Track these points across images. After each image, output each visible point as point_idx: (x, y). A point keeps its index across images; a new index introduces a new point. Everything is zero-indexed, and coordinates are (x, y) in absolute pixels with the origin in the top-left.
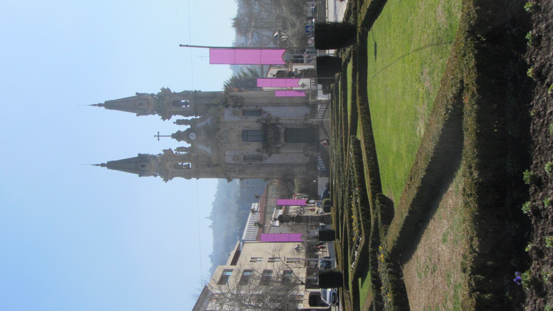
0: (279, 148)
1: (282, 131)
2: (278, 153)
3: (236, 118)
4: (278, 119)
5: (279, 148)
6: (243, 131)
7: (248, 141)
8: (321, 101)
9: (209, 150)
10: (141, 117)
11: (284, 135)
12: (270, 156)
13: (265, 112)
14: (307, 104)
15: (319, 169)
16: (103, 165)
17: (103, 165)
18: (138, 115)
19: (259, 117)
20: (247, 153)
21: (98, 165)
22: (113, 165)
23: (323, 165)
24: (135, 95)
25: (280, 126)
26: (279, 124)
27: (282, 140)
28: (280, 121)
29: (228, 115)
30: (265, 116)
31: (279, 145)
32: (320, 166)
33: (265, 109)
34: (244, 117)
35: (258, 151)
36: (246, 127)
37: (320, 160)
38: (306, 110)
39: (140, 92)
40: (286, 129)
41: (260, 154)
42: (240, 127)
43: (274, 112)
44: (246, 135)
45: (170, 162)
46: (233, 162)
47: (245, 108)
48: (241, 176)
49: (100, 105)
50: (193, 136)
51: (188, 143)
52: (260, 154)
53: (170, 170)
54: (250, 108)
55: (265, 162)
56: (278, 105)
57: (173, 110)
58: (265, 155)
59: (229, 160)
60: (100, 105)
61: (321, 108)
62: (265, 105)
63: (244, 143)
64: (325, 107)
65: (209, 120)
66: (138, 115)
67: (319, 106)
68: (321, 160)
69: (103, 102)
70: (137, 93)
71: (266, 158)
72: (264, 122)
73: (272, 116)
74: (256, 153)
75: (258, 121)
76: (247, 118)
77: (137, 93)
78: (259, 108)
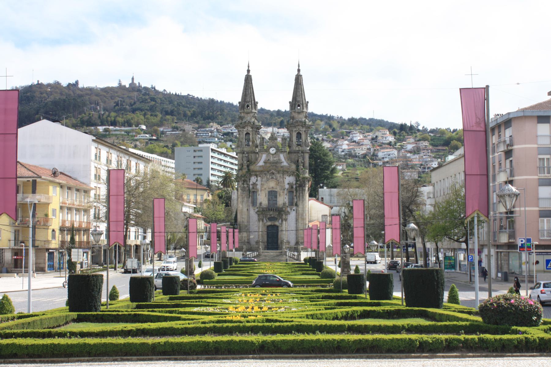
0: (263, 221)
1: (277, 223)
2: (259, 220)
3: (287, 186)
4: (286, 220)
5: (263, 221)
6: (276, 192)
8: (300, 255)
9: (261, 163)
10: (289, 105)
12: (256, 213)
14: (297, 243)
15: (248, 253)
16: (248, 71)
17: (248, 71)
18: (290, 102)
19: (287, 204)
21: (249, 67)
22: (248, 80)
24: (307, 100)
25: (280, 221)
26: (282, 221)
27: (269, 223)
28: (284, 222)
29: (289, 179)
30: (289, 209)
31: (265, 221)
35: (261, 204)
39: (309, 104)
40: (277, 227)
41: (258, 205)
43: (292, 216)
44: (273, 195)
45: (251, 130)
46: (251, 183)
48: (239, 189)
49: (299, 70)
50: (272, 151)
51: (267, 147)
52: (258, 205)
56: (297, 220)
58: (257, 210)
59: (253, 179)
60: (299, 70)
63: (267, 192)
65: (285, 164)
66: (290, 102)
67: (296, 254)
69: (301, 73)
70: (308, 102)
72: (284, 209)
74: (258, 202)
75: (284, 204)
77: (308, 102)
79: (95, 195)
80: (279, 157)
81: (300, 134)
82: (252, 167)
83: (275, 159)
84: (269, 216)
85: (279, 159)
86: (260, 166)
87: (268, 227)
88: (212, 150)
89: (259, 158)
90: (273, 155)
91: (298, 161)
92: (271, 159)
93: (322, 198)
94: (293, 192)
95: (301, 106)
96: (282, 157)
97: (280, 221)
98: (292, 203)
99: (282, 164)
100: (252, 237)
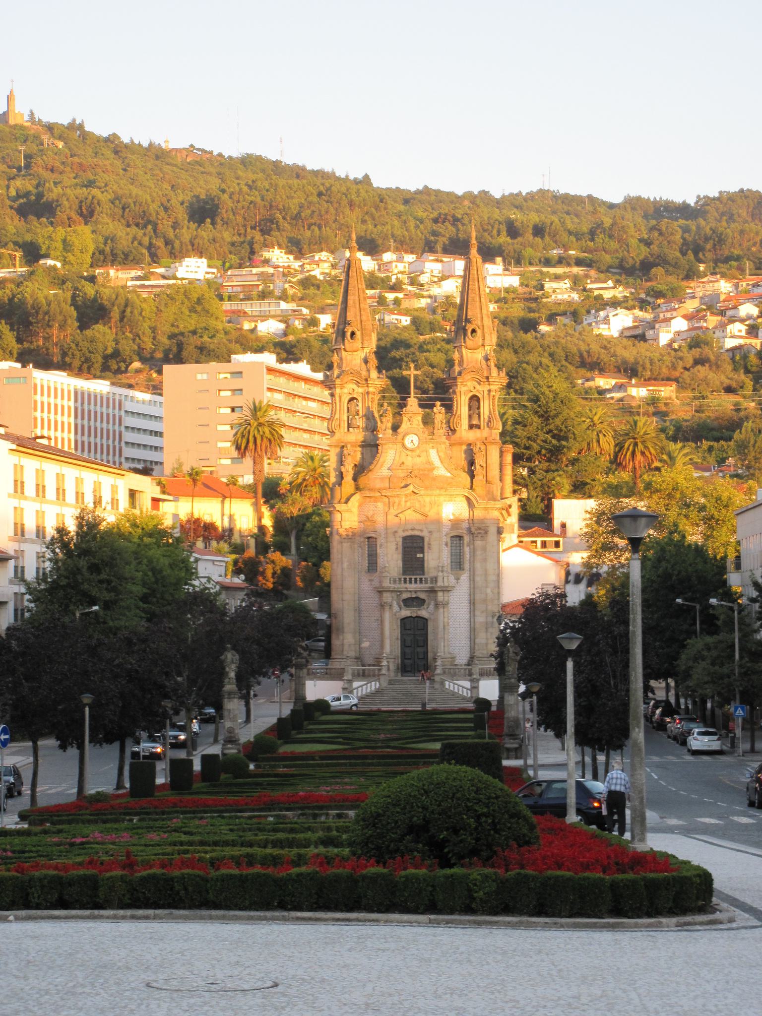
1: (423, 613)
2: (382, 606)
4: (445, 605)
6: (422, 539)
7: (404, 548)
11: (414, 615)
13: (458, 579)
14: (472, 658)
15: (356, 684)
20: (381, 546)
23: (364, 693)
26: (437, 605)
27: (406, 613)
28: (441, 610)
31: (396, 607)
32: (361, 686)
33: (465, 577)
34: (449, 541)
36: (429, 544)
37: (374, 686)
38: (462, 658)
40: (426, 620)
42: (430, 532)
47: (467, 539)
53: (346, 391)
54: (467, 550)
55: (365, 578)
56: (472, 603)
57: (463, 397)
61: (463, 687)
62: (472, 579)
63: (400, 540)
64: (465, 694)
67: (467, 684)
68: (373, 688)
71: (371, 580)
73: (451, 593)
74: (381, 561)
76: (446, 545)
78: (467, 566)
79: (16, 567)
80: (428, 456)
81: (478, 400)
82: (362, 481)
83: (418, 460)
84: (405, 596)
85: (429, 463)
86: (382, 479)
87: (404, 620)
88: (270, 370)
89: (381, 460)
90: (412, 450)
91: (471, 463)
92: (409, 461)
93: (563, 526)
94: (460, 537)
95: (479, 332)
96: (433, 454)
97: (432, 606)
98: (458, 564)
99: (435, 472)
100: (366, 644)
